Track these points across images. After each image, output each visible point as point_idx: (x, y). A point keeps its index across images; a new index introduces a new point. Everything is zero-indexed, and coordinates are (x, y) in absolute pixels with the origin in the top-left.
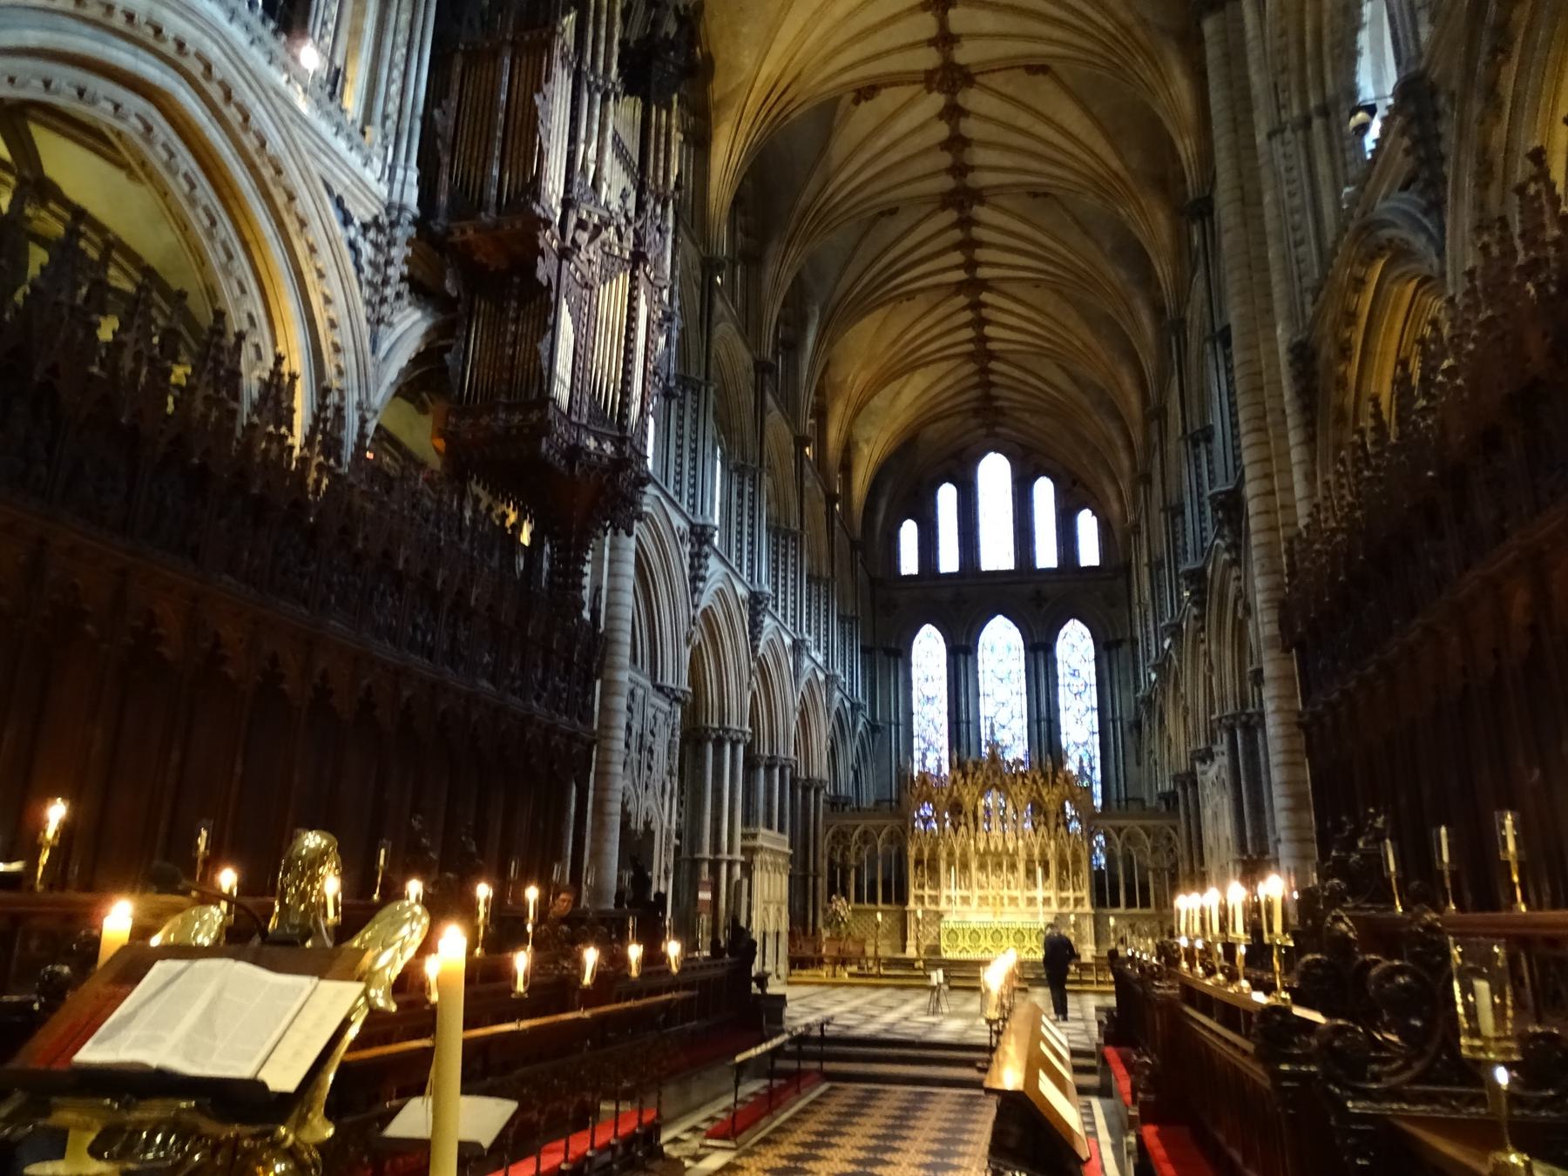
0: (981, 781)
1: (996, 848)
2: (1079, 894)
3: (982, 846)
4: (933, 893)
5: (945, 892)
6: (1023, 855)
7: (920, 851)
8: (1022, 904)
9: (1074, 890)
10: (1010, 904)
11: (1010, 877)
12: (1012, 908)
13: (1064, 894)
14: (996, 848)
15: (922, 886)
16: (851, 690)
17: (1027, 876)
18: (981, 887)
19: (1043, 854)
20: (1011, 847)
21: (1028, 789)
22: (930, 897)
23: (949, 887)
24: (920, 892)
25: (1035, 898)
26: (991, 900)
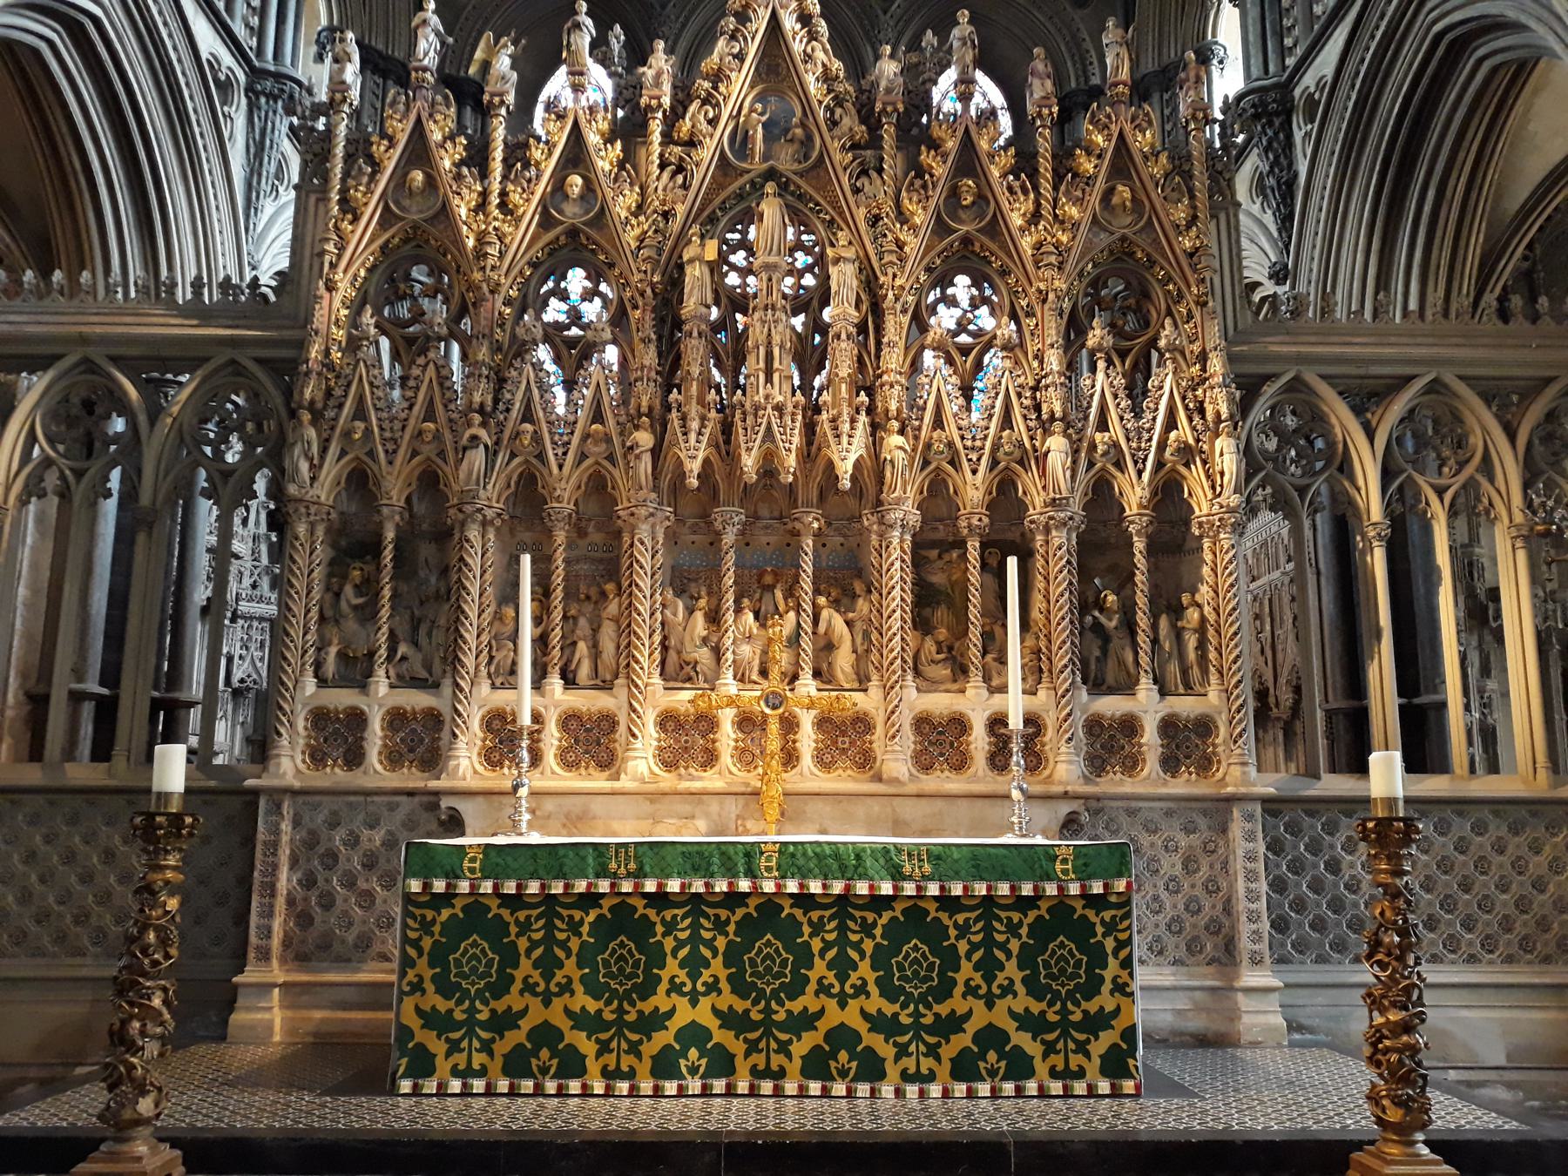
0: (706, 153)
1: (769, 471)
2: (1185, 706)
3: (694, 455)
4: (417, 700)
5: (481, 698)
6: (905, 505)
7: (360, 482)
8: (897, 759)
9: (1163, 693)
10: (823, 761)
11: (834, 621)
12: (842, 780)
13: (1110, 706)
14: (769, 471)
15: (356, 671)
16: (260, 33)
17: (922, 624)
18: (677, 671)
19: (1005, 497)
20: (847, 455)
21: (937, 196)
22: (396, 718)
23: (506, 676)
24: (342, 698)
25: (959, 724)
26: (727, 735)
